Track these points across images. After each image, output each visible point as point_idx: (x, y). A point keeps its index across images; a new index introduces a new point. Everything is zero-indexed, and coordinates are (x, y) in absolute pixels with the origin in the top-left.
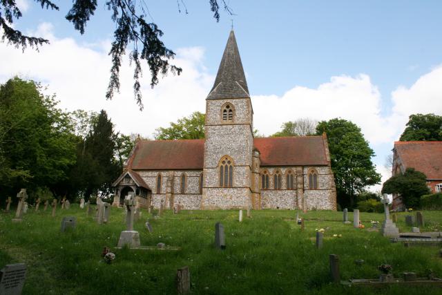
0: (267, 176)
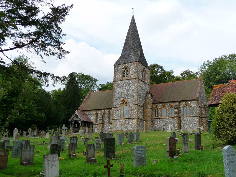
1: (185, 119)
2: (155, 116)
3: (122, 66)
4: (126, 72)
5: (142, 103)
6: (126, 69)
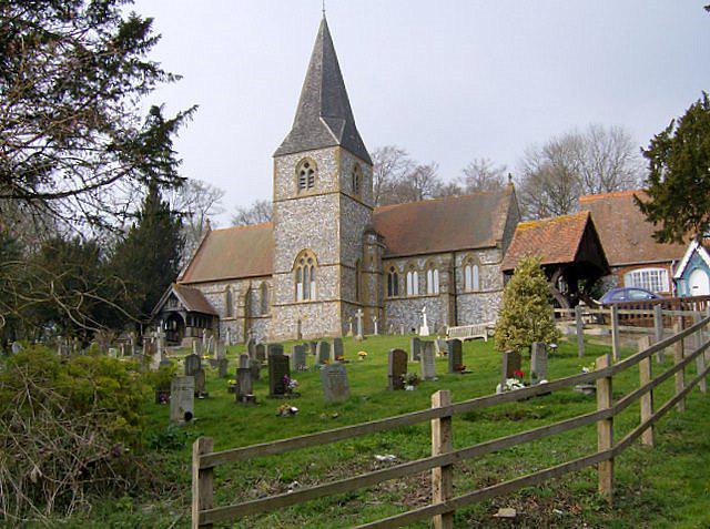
0: (396, 275)
1: (469, 298)
3: (297, 158)
4: (306, 176)
6: (307, 165)
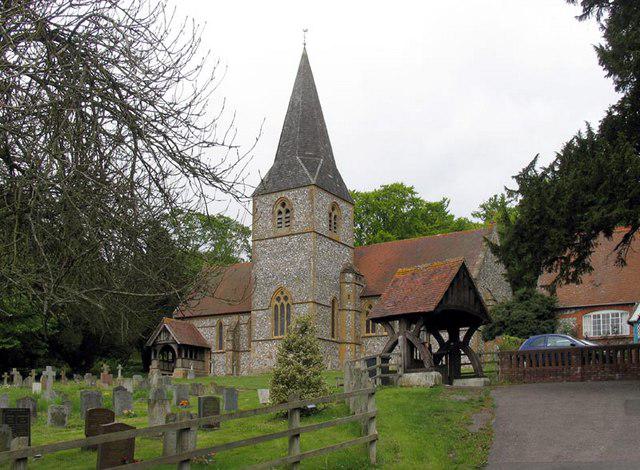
2: (368, 331)
3: (274, 197)
5: (330, 299)
6: (283, 205)
